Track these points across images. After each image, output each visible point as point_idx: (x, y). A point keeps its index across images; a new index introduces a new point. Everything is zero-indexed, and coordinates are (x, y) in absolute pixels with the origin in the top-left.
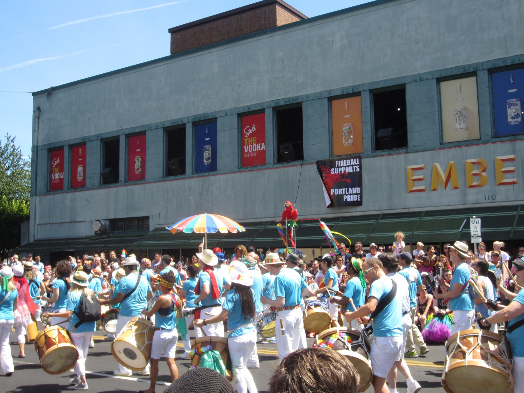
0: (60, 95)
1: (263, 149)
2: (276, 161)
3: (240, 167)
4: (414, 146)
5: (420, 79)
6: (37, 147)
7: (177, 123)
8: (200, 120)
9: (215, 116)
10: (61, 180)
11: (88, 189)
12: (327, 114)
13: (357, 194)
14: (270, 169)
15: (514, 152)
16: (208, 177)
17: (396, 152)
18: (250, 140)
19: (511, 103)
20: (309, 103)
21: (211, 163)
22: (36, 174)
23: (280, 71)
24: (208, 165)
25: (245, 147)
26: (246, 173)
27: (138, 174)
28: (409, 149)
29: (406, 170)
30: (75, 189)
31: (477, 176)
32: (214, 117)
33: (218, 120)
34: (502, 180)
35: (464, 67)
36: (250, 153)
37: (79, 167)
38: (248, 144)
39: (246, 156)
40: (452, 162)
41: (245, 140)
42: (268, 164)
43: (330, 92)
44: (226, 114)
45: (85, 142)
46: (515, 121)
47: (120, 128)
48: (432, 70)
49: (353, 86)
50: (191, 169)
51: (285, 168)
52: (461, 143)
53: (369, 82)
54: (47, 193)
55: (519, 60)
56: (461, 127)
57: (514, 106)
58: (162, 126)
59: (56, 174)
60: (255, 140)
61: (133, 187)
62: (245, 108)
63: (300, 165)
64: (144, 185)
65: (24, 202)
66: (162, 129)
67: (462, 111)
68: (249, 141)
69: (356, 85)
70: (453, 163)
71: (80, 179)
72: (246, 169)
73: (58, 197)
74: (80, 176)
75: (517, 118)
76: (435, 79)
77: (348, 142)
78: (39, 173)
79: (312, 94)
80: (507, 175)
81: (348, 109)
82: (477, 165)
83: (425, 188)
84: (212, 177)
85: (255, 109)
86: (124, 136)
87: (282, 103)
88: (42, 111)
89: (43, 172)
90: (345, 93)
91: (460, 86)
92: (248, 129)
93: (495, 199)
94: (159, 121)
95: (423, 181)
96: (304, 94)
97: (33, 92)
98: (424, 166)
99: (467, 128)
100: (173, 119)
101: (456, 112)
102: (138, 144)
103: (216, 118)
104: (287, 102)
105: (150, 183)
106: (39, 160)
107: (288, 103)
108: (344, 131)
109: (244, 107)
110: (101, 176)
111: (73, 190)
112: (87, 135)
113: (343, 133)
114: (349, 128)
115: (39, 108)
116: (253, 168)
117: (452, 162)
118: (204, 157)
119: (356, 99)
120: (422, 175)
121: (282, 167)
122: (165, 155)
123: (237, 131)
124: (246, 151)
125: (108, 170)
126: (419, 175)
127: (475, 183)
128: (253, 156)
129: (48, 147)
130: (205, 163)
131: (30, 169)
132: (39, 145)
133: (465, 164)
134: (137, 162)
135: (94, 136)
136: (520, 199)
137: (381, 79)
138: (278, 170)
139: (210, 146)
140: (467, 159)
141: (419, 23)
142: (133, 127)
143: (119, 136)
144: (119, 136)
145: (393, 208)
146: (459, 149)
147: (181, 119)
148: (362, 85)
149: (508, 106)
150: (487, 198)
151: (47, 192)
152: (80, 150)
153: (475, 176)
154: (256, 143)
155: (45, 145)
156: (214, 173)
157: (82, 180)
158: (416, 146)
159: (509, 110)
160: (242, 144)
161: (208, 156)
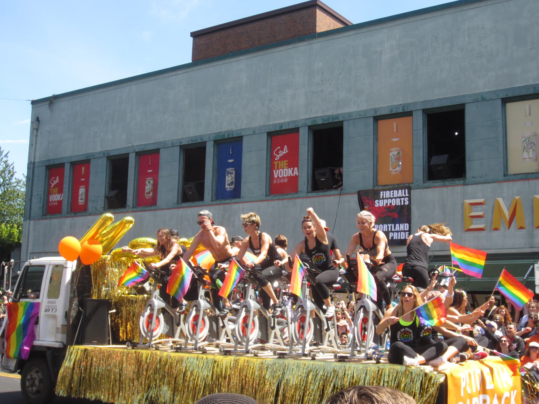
0: (62, 104)
1: (296, 174)
2: (310, 189)
3: (267, 194)
4: (473, 177)
5: (482, 99)
6: (34, 163)
7: (197, 141)
8: (223, 138)
9: (241, 134)
10: (60, 202)
11: (90, 215)
12: (372, 137)
13: (405, 231)
14: (303, 198)
17: (451, 183)
18: (281, 163)
21: (234, 189)
22: (32, 195)
23: (319, 84)
24: (231, 191)
25: (274, 171)
26: (275, 202)
27: (149, 199)
28: (467, 181)
29: (463, 204)
30: (75, 213)
32: (240, 135)
33: (245, 140)
35: (534, 87)
36: (280, 179)
37: (80, 188)
38: (278, 169)
39: (275, 182)
40: (517, 198)
41: (275, 164)
42: (301, 192)
43: (377, 111)
44: (254, 133)
45: (90, 159)
47: (131, 145)
48: (497, 89)
49: (403, 104)
50: (210, 196)
51: (320, 198)
52: (529, 175)
53: (422, 100)
54: (43, 217)
56: (529, 156)
58: (178, 144)
59: (54, 195)
60: (287, 164)
61: (142, 213)
62: (276, 126)
63: (338, 195)
64: (155, 211)
65: (16, 226)
66: (179, 147)
67: (530, 138)
68: (280, 165)
69: (407, 104)
70: (519, 198)
71: (81, 202)
72: (275, 198)
73: (55, 222)
74: (82, 199)
76: (501, 99)
77: (395, 170)
78: (35, 193)
79: (356, 112)
81: (397, 131)
83: (485, 227)
84: (235, 204)
85: (287, 128)
86: (134, 154)
87: (320, 122)
88: (41, 122)
89: (39, 193)
90: (394, 112)
91: (530, 108)
92: (278, 150)
94: (175, 138)
95: (483, 219)
96: (345, 112)
97: (32, 100)
98: (485, 201)
99: (537, 158)
100: (191, 136)
101: (524, 139)
102: (150, 163)
103: (242, 137)
104: (326, 121)
105: (162, 209)
106: (35, 179)
107: (327, 122)
108: (391, 157)
109: (273, 125)
110: (106, 200)
111: (73, 215)
112: (92, 152)
113: (390, 159)
114: (398, 153)
115: (38, 118)
116: (283, 196)
117: (517, 198)
118: (226, 181)
119: (406, 120)
120: (481, 211)
121: (317, 197)
122: (180, 177)
123: (265, 153)
124: (276, 176)
125: (114, 193)
126: (478, 211)
128: (284, 182)
129: (47, 164)
130: (227, 188)
131: (23, 190)
132: (36, 161)
133: (532, 200)
134: (148, 184)
135: (100, 153)
137: (437, 98)
138: (312, 199)
139: (234, 169)
140: (535, 194)
141: (483, 33)
142: (145, 145)
143: (128, 154)
144: (128, 154)
146: (527, 182)
147: (201, 137)
148: (414, 104)
151: (43, 215)
152: (83, 168)
154: (287, 167)
155: (43, 161)
156: (238, 200)
157: (83, 204)
158: (476, 177)
160: (271, 167)
161: (231, 181)
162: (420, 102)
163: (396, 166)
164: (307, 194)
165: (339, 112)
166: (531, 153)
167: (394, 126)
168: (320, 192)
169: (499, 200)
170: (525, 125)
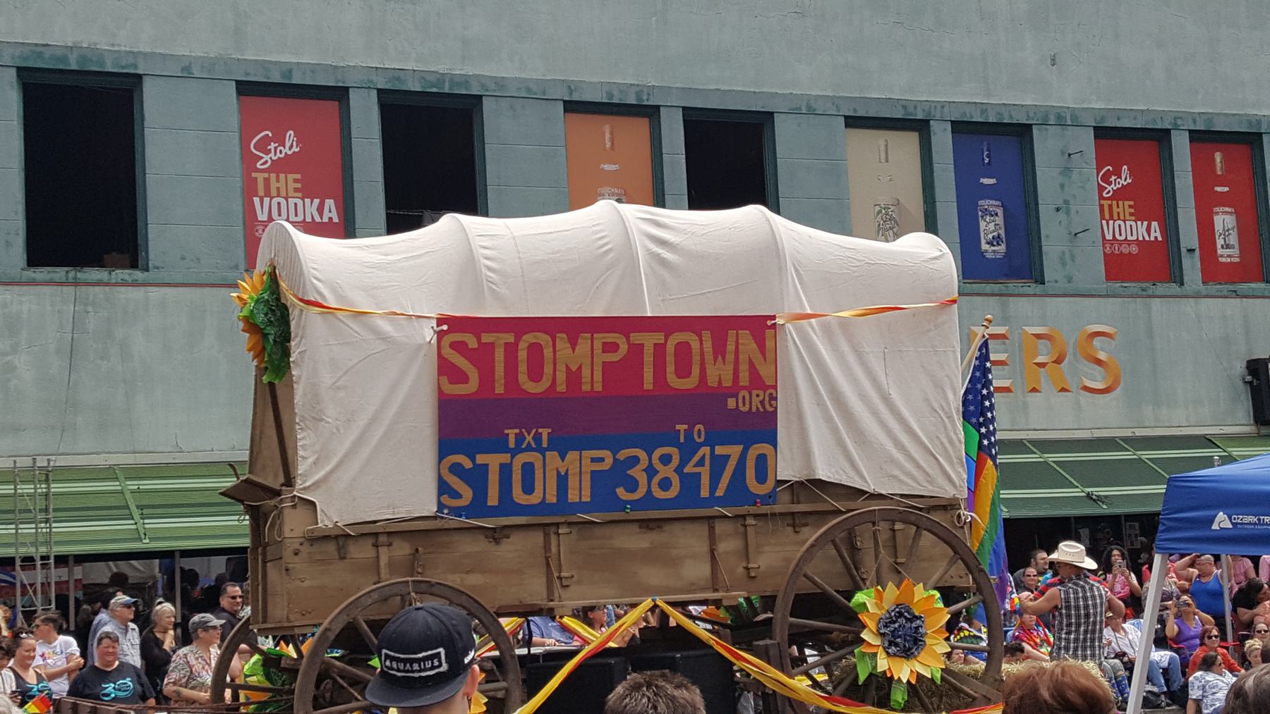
15: (1005, 320)
16: (107, 287)
19: (986, 209)
20: (504, 103)
53: (679, 85)
55: (1011, 117)
75: (999, 244)
81: (612, 148)
85: (308, 81)
90: (615, 100)
91: (886, 145)
101: (878, 208)
104: (432, 87)
107: (434, 90)
136: (1021, 428)
149: (980, 213)
156: (138, 275)
159: (982, 224)
162: (677, 88)
165: (470, 70)
167: (604, 134)
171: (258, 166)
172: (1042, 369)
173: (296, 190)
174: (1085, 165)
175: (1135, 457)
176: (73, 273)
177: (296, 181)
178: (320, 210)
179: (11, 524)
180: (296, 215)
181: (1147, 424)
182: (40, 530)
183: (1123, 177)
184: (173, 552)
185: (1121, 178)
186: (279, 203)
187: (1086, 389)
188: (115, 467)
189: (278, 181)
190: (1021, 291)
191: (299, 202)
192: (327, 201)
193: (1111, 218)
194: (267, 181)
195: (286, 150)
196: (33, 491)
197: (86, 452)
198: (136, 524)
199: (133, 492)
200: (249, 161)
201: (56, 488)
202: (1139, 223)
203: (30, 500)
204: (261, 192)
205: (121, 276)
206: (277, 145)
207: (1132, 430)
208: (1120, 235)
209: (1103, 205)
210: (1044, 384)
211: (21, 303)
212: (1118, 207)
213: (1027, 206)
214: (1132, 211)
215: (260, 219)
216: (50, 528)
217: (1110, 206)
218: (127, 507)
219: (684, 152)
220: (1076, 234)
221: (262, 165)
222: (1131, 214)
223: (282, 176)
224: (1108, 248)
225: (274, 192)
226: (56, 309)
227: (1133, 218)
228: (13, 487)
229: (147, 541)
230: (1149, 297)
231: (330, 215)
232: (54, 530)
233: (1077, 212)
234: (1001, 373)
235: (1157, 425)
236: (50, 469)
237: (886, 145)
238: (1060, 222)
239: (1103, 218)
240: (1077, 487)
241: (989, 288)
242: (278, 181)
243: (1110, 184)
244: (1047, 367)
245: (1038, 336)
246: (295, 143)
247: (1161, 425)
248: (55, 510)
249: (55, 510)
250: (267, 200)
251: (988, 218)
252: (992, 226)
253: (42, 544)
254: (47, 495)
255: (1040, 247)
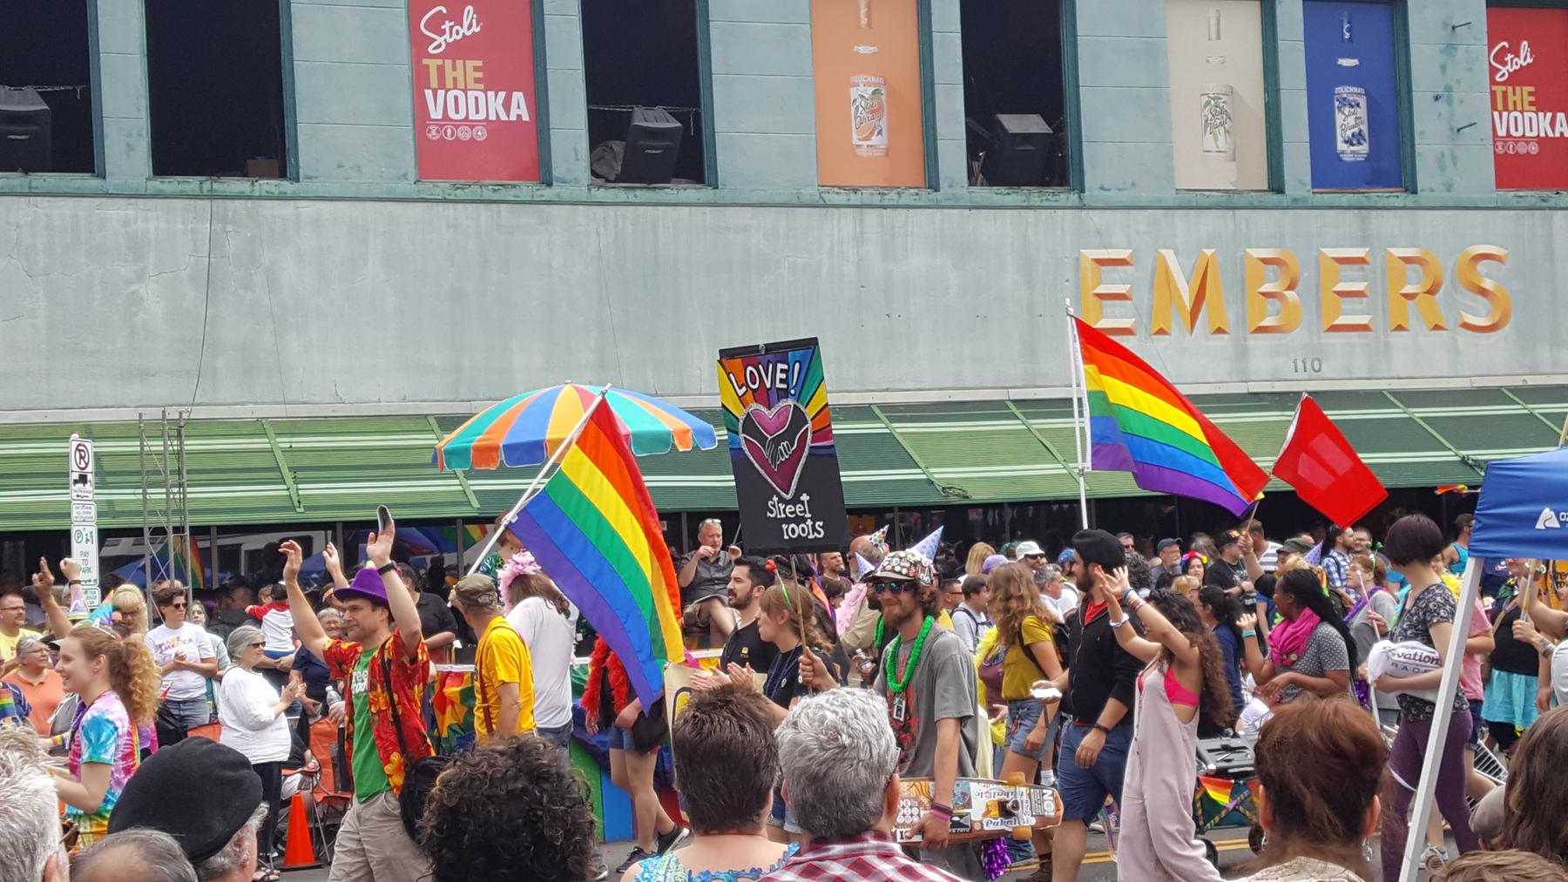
4: (1102, 188)
16: (249, 202)
17: (1048, 200)
19: (1344, 99)
31: (1275, 300)
34: (1336, 317)
40: (1209, 252)
46: (1353, 152)
57: (1352, 107)
70: (1213, 254)
72: (459, 191)
75: (1359, 143)
80: (1348, 303)
81: (869, 25)
82: (1275, 267)
91: (1218, 20)
93: (1319, 371)
95: (1127, 302)
99: (1234, 152)
101: (1205, 99)
108: (855, 101)
113: (853, 109)
114: (873, 93)
127: (1268, 322)
145: (1039, 383)
149: (1337, 104)
150: (1300, 365)
153: (1271, 300)
156: (286, 186)
159: (1339, 118)
163: (872, 133)
164: (589, 190)
166: (1221, 138)
168: (639, 188)
169: (1167, 257)
170: (1208, 61)
171: (431, 50)
172: (1411, 302)
173: (477, 80)
174: (1473, 42)
175: (1526, 411)
176: (209, 183)
177: (476, 69)
178: (507, 105)
179: (140, 488)
180: (477, 112)
181: (1541, 370)
182: (172, 496)
183: (1522, 56)
184: (335, 522)
185: (1518, 55)
186: (456, 98)
187: (1467, 326)
188: (264, 421)
189: (454, 68)
190: (1386, 202)
191: (481, 95)
192: (514, 93)
193: (1506, 108)
194: (441, 70)
195: (464, 31)
196: (162, 448)
197: (229, 401)
198: (288, 489)
199: (284, 451)
200: (419, 44)
201: (191, 445)
202: (1541, 114)
203: (160, 460)
204: (434, 83)
205: (266, 188)
206: (452, 23)
207: (1524, 377)
208: (1517, 130)
209: (1495, 92)
210: (1412, 323)
211: (147, 220)
212: (1514, 94)
213: (1397, 94)
214: (1532, 99)
215: (433, 117)
216: (184, 493)
217: (1505, 94)
218: (278, 469)
219: (960, 30)
220: (1459, 130)
221: (435, 48)
222: (1531, 104)
223: (459, 63)
224: (1500, 148)
225: (449, 84)
226: (189, 228)
227: (1534, 108)
228: (138, 443)
229: (302, 510)
230: (1551, 208)
231: (518, 112)
232: (188, 496)
233: (1462, 102)
234: (1357, 306)
235: (1556, 371)
236: (182, 424)
237: (1218, 20)
238: (1440, 114)
239: (1494, 108)
240: (1450, 449)
241: (1346, 199)
242: (454, 68)
243: (1504, 64)
244: (1417, 299)
245: (1407, 260)
246: (474, 21)
247: (1560, 371)
248: (189, 472)
249: (189, 472)
250: (441, 93)
251: (1347, 110)
252: (1351, 120)
253: (175, 512)
254: (179, 454)
255: (1413, 146)
